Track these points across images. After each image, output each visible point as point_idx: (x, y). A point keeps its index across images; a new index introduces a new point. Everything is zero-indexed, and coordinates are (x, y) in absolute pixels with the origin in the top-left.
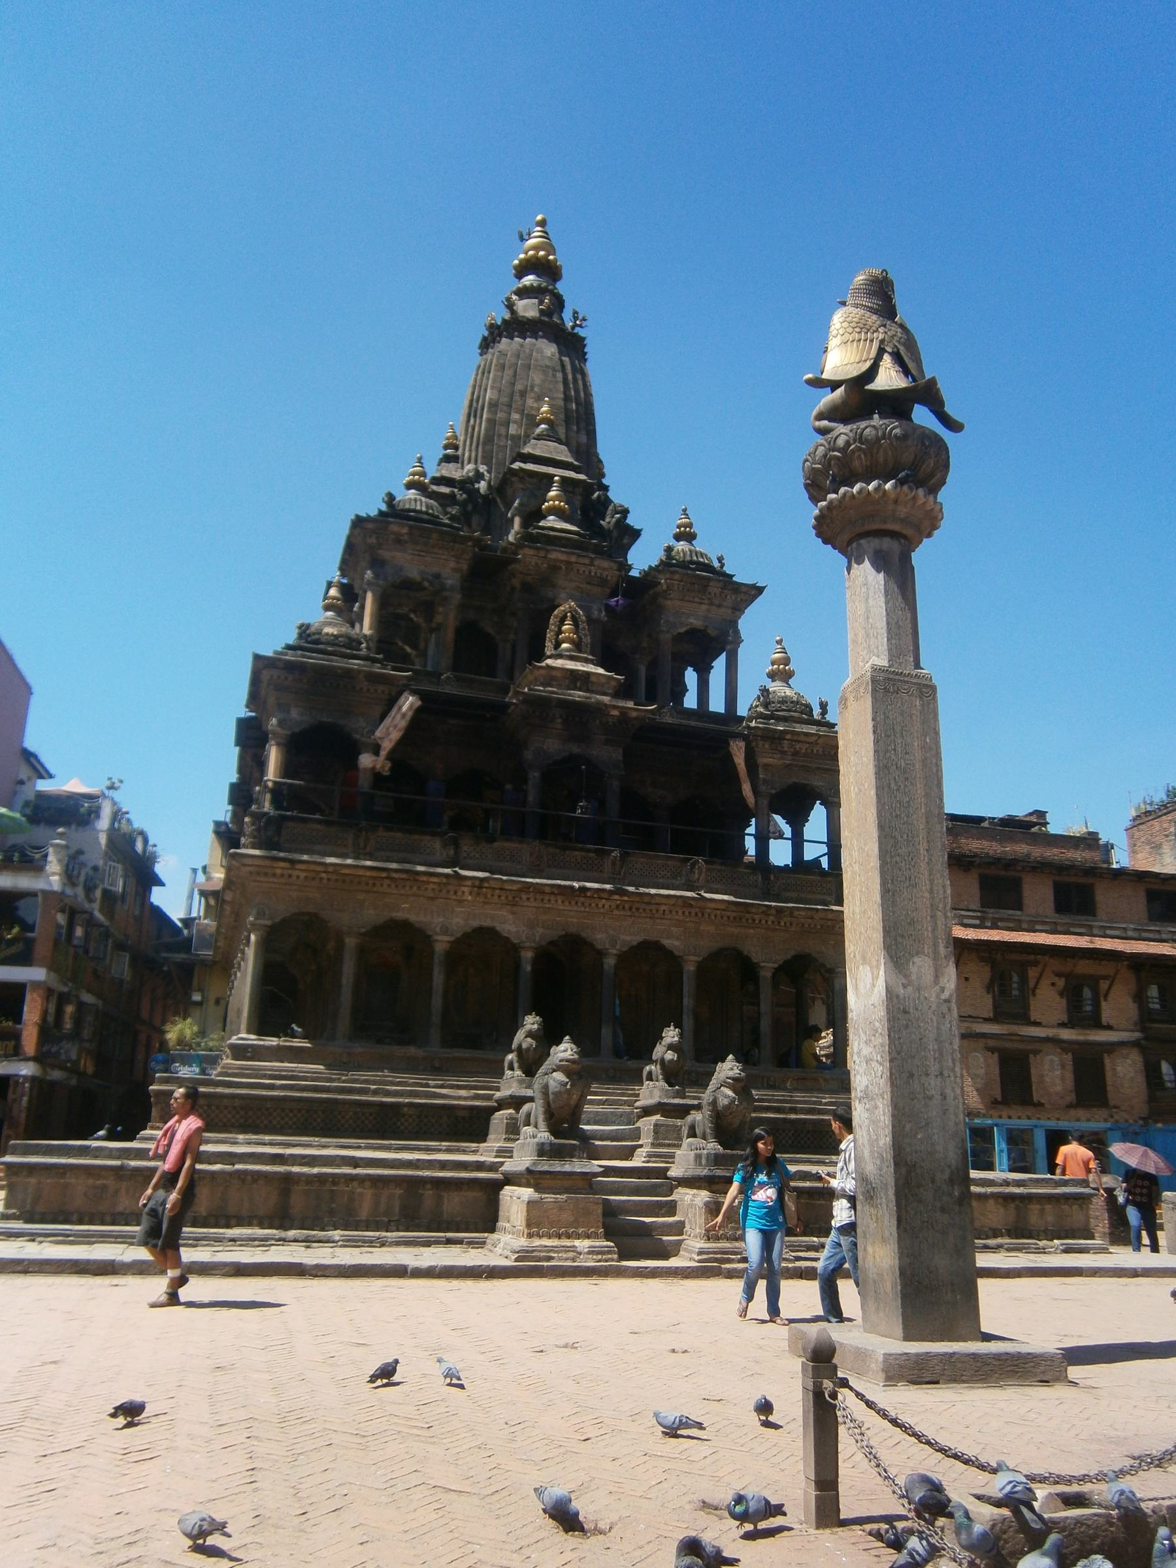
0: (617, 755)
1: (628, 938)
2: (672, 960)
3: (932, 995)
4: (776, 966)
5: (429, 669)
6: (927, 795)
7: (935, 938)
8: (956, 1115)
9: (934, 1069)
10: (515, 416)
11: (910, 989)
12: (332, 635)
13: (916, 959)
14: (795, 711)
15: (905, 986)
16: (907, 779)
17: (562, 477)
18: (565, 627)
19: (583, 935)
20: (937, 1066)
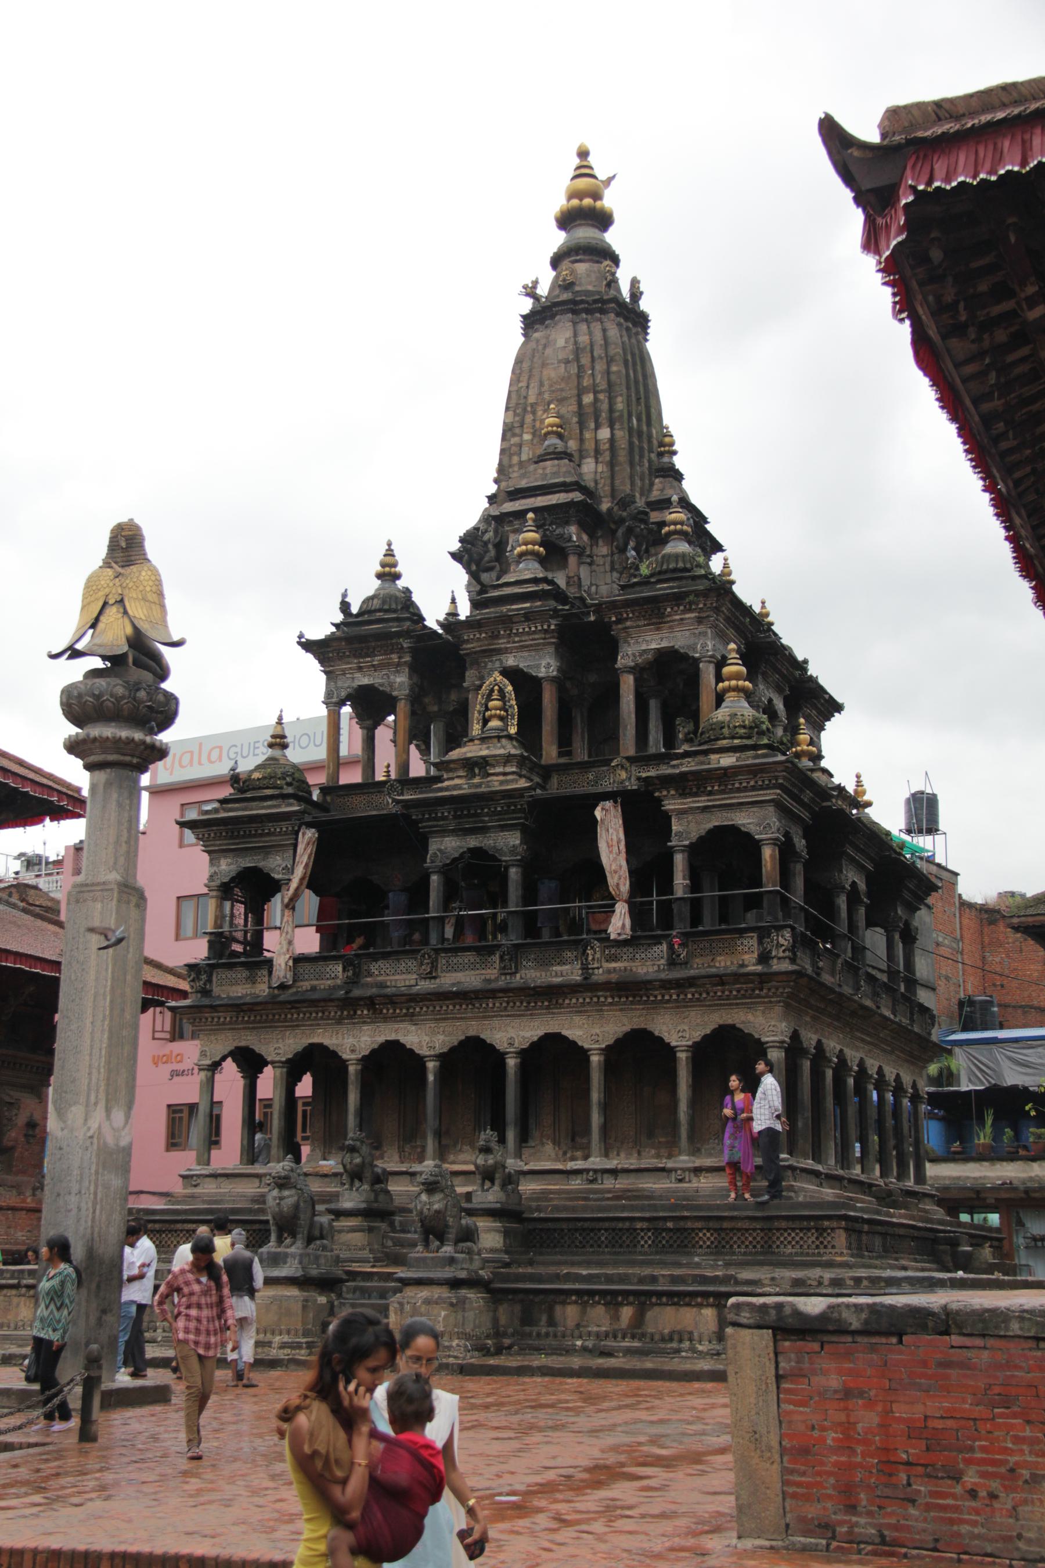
0: (513, 839)
1: (528, 1034)
2: (577, 1054)
3: (81, 1137)
4: (690, 1043)
5: (380, 777)
6: (97, 979)
7: (89, 1089)
8: (86, 1222)
9: (75, 1190)
10: (527, 437)
11: (66, 1131)
12: (258, 779)
13: (73, 1108)
14: (724, 738)
15: (62, 1129)
16: (83, 970)
17: (535, 510)
18: (491, 704)
19: (482, 1036)
20: (77, 1187)
